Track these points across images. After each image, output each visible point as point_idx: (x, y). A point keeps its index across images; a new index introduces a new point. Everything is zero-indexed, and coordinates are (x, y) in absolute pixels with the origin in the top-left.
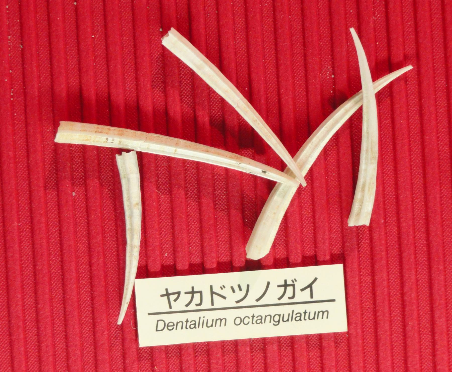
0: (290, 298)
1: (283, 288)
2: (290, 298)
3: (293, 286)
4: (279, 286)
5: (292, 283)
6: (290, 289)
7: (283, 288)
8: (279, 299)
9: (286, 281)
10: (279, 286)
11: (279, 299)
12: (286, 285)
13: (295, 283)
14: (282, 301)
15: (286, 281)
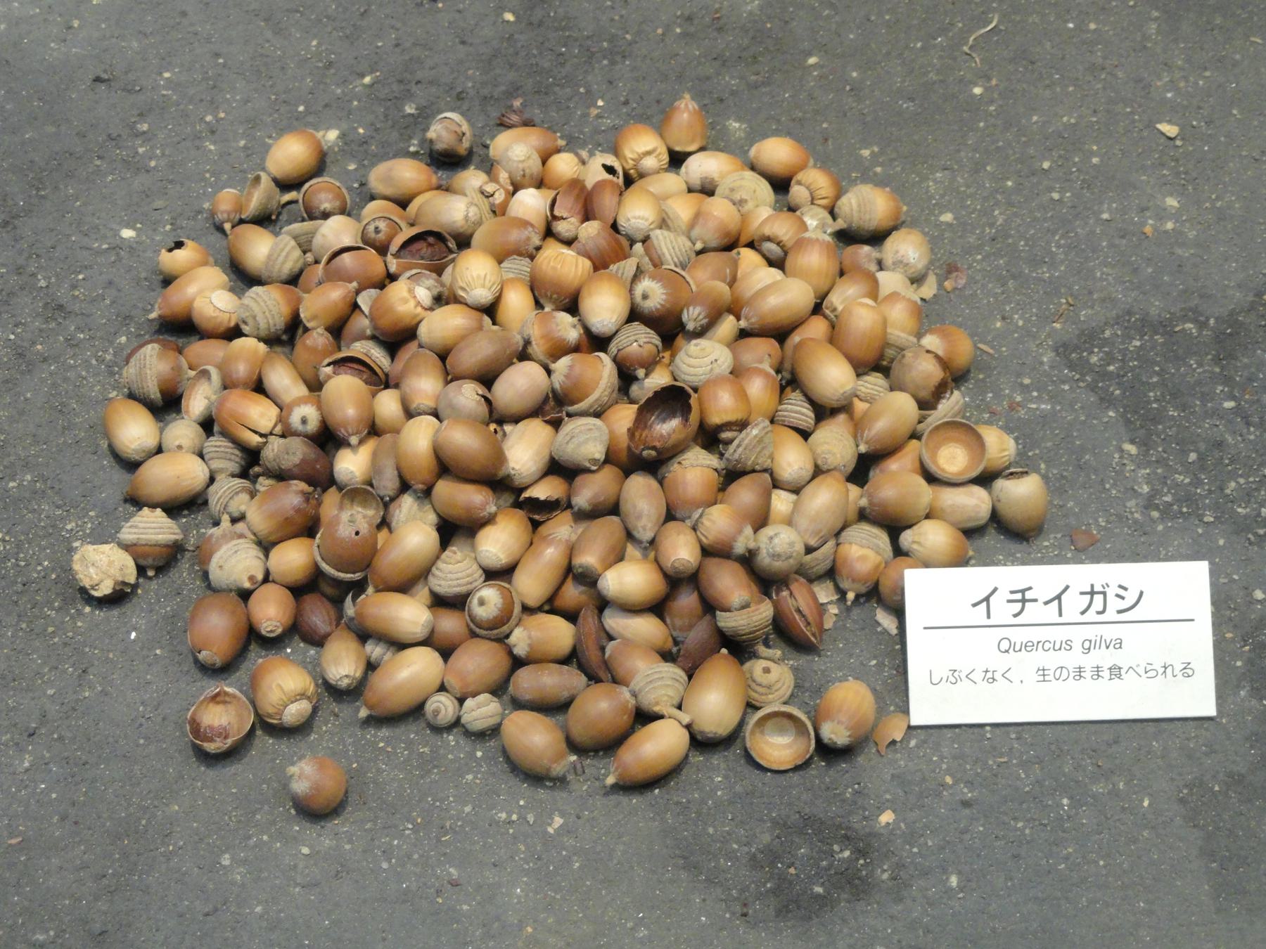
0: (1099, 613)
1: (1089, 596)
2: (1099, 613)
3: (1104, 594)
4: (1082, 593)
5: (1102, 590)
6: (1098, 599)
7: (1089, 596)
8: (1083, 613)
9: (1092, 586)
10: (1082, 593)
11: (1083, 613)
12: (1092, 593)
13: (1107, 589)
14: (1086, 618)
15: (1092, 586)
